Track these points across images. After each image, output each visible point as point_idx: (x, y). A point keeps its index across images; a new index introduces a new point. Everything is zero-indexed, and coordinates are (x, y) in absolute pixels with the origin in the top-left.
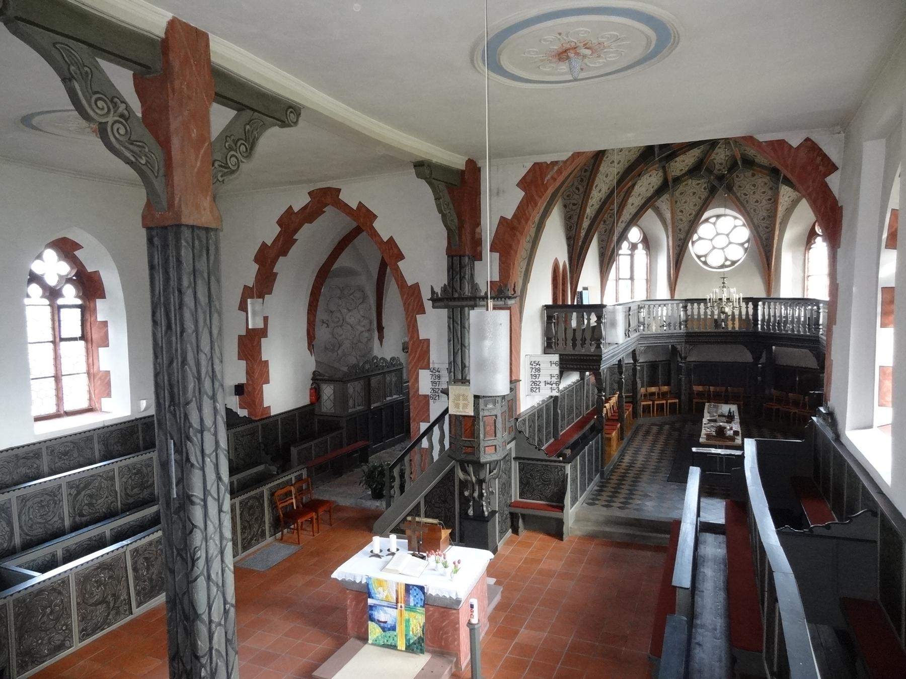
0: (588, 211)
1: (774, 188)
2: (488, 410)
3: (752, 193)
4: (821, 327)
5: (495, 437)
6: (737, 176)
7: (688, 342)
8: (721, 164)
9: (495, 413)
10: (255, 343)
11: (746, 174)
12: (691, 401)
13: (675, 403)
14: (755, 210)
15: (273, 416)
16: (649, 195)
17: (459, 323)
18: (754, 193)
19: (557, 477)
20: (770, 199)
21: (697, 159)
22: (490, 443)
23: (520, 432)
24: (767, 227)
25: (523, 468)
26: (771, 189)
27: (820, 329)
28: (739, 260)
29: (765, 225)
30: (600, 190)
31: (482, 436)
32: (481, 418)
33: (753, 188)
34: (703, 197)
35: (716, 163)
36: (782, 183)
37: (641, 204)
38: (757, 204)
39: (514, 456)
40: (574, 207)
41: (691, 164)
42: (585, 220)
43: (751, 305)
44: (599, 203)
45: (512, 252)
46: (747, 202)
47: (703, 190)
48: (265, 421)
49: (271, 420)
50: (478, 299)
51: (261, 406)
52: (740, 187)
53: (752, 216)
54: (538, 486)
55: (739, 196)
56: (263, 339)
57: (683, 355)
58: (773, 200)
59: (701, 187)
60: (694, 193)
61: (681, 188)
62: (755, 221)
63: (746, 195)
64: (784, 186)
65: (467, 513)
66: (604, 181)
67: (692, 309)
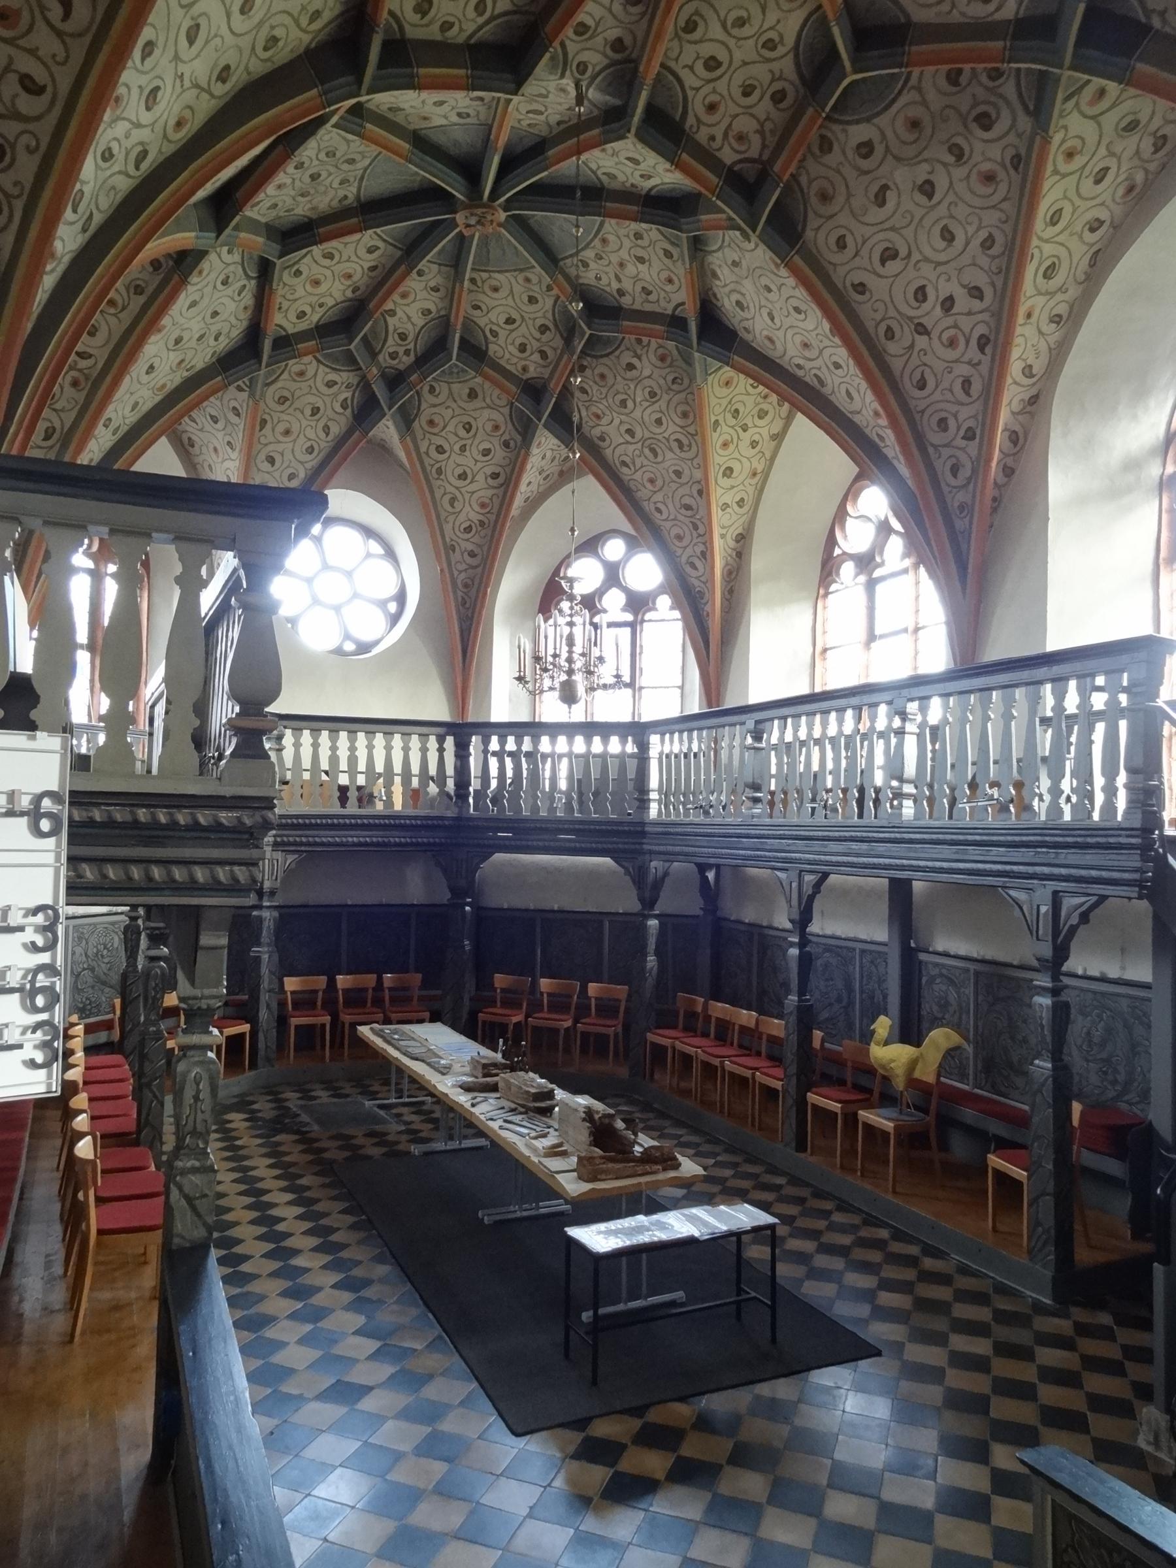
0: (89, 168)
1: (512, 444)
3: (457, 448)
4: (654, 796)
6: (432, 390)
7: (283, 844)
8: (403, 337)
11: (455, 387)
12: (282, 1021)
13: (242, 1035)
14: (452, 501)
16: (201, 358)
18: (463, 449)
20: (495, 476)
21: (349, 294)
24: (472, 554)
26: (506, 444)
27: (649, 800)
28: (376, 643)
29: (470, 547)
30: (156, 89)
33: (462, 433)
34: (335, 430)
35: (391, 329)
36: (546, 426)
37: (170, 386)
38: (460, 483)
40: (27, 104)
41: (330, 302)
42: (68, 214)
43: (450, 742)
44: (131, 170)
46: (439, 471)
47: (341, 410)
52: (431, 423)
53: (443, 515)
55: (423, 449)
57: (267, 885)
58: (501, 480)
59: (336, 395)
60: (315, 411)
61: (285, 383)
62: (448, 528)
63: (440, 450)
64: (546, 433)
66: (177, 58)
67: (297, 745)
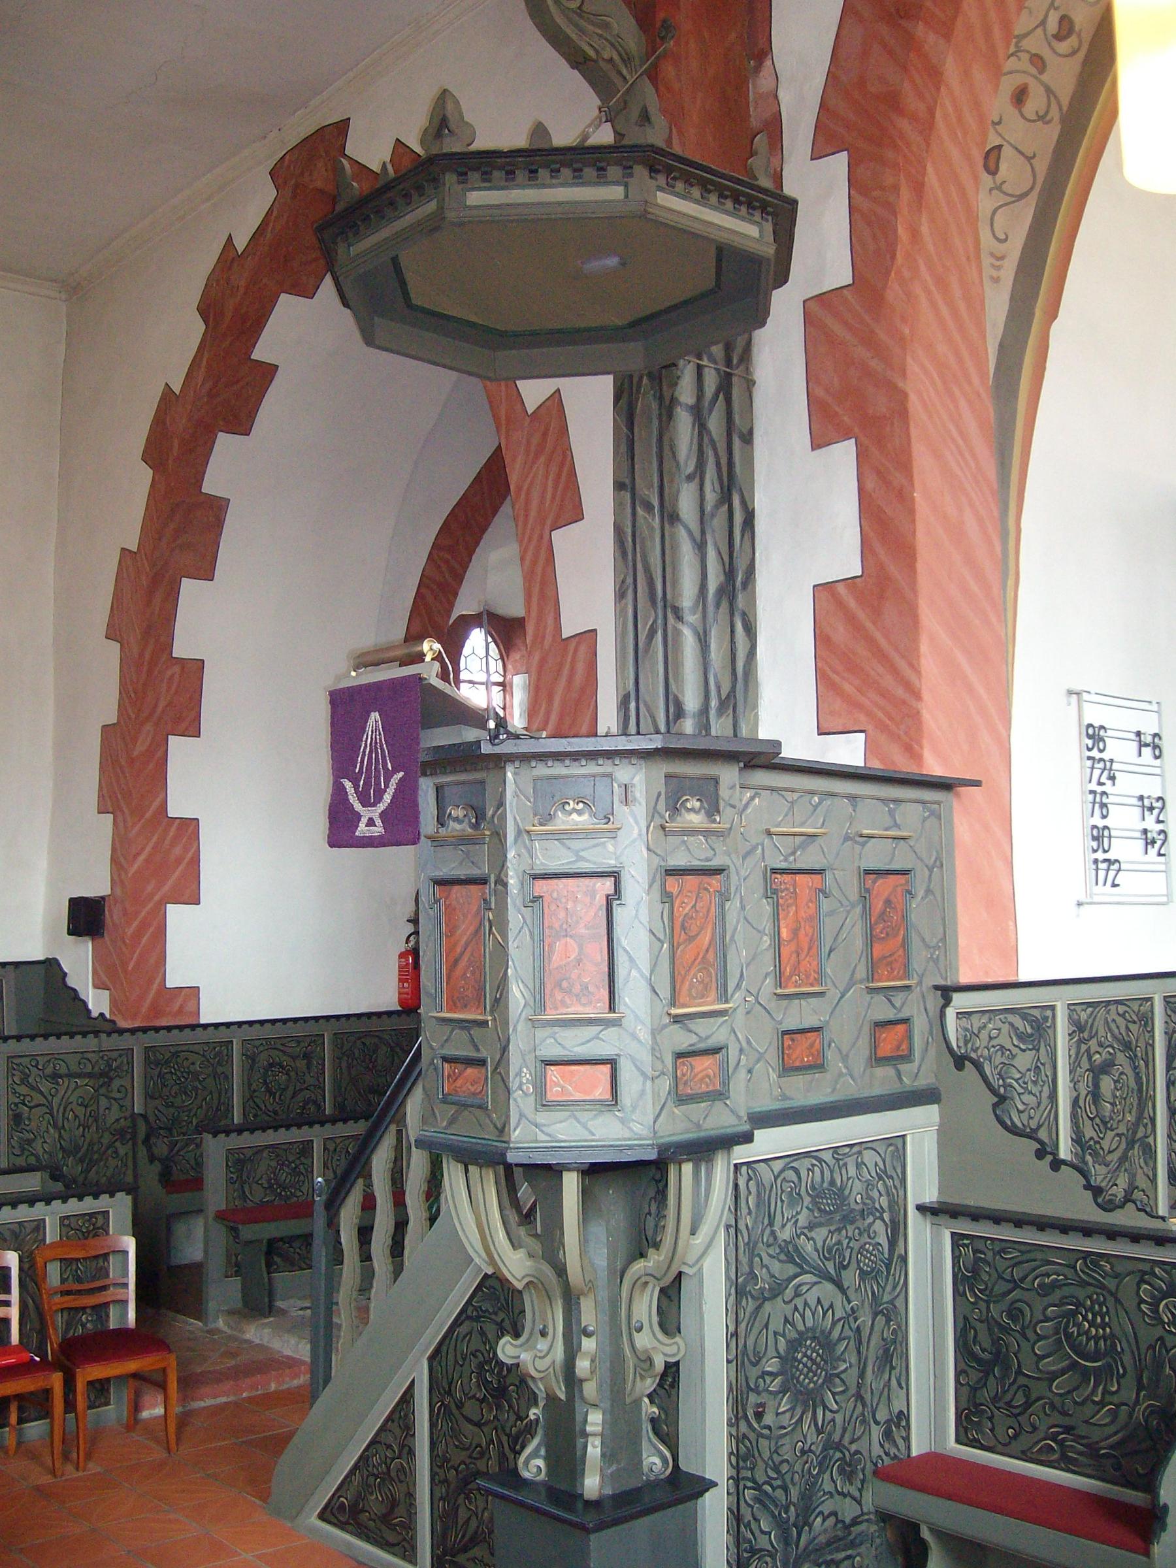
2: (562, 836)
5: (612, 1008)
9: (610, 863)
10: (140, 747)
15: (205, 1026)
17: (655, 502)
19: (1148, 1335)
22: (574, 1043)
23: (960, 1062)
25: (975, 1271)
31: (518, 994)
32: (512, 882)
39: (930, 1196)
45: (904, 124)
48: (160, 1039)
49: (201, 1036)
50: (450, 179)
51: (150, 982)
54: (1053, 1377)
56: (176, 743)
65: (512, 1477)
